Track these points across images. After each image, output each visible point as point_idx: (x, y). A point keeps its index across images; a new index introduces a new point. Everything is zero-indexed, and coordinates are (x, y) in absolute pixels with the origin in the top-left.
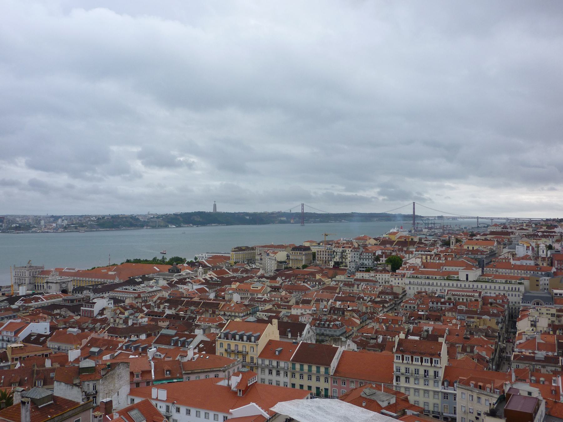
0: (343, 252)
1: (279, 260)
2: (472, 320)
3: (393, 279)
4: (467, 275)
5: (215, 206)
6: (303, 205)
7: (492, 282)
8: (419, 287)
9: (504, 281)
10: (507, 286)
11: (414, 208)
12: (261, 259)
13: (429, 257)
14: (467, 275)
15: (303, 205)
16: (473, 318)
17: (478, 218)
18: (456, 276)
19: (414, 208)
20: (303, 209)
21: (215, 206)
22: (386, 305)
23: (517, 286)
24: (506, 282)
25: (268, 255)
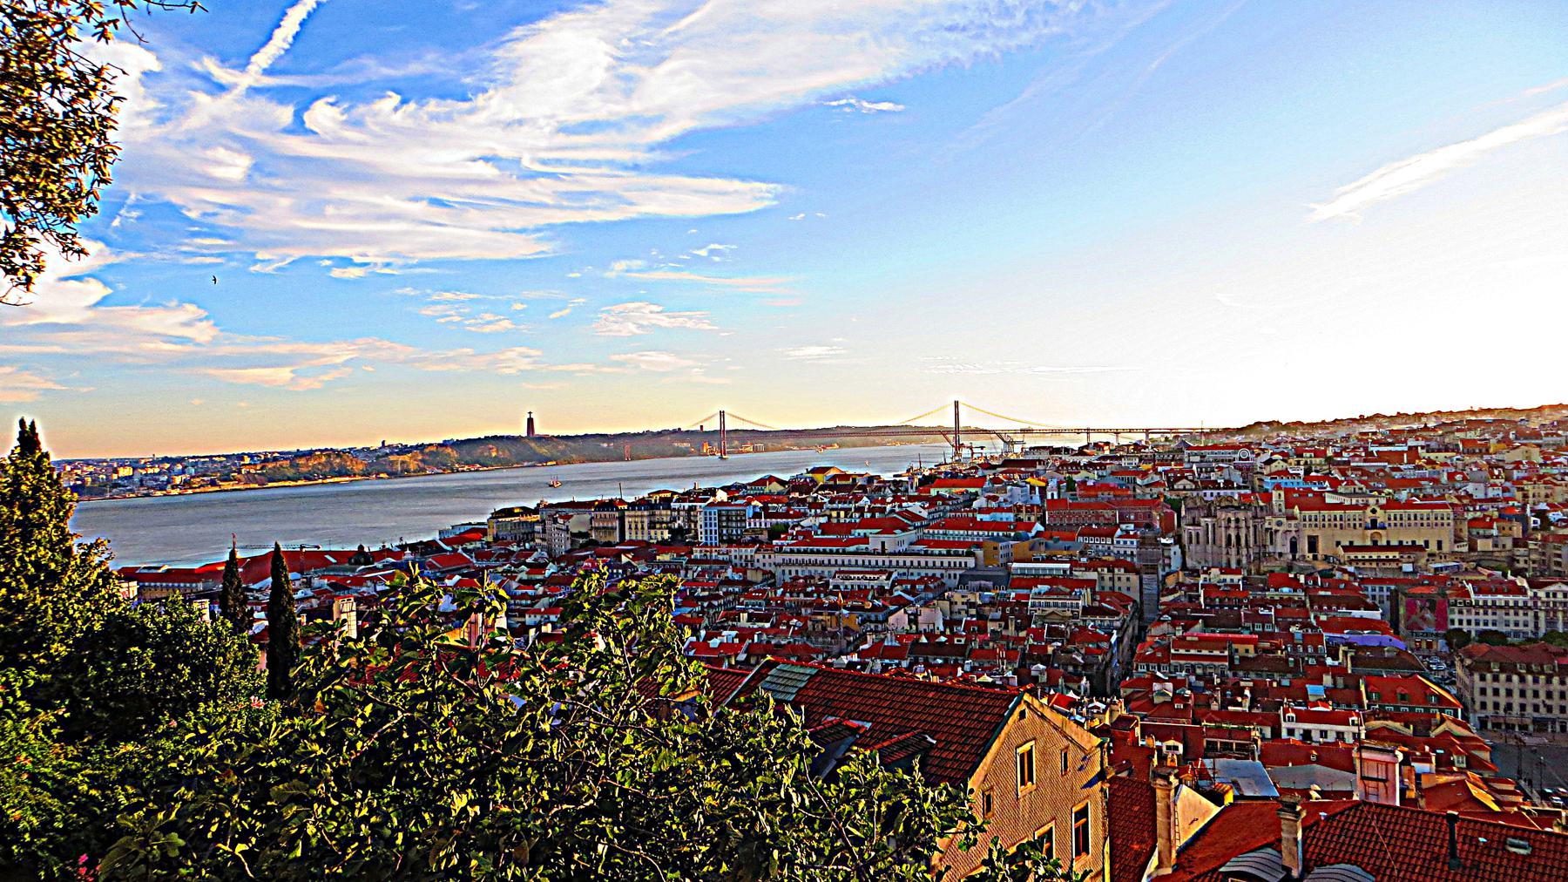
0: (691, 509)
1: (575, 531)
2: (819, 618)
3: (759, 556)
4: (883, 543)
5: (530, 421)
6: (722, 414)
7: (926, 554)
8: (793, 569)
9: (944, 551)
10: (946, 560)
11: (957, 415)
12: (544, 531)
13: (842, 513)
14: (883, 543)
15: (722, 414)
16: (821, 614)
17: (1088, 431)
18: (863, 546)
19: (957, 415)
20: (722, 423)
21: (530, 421)
22: (716, 603)
23: (963, 560)
24: (949, 554)
25: (555, 521)
